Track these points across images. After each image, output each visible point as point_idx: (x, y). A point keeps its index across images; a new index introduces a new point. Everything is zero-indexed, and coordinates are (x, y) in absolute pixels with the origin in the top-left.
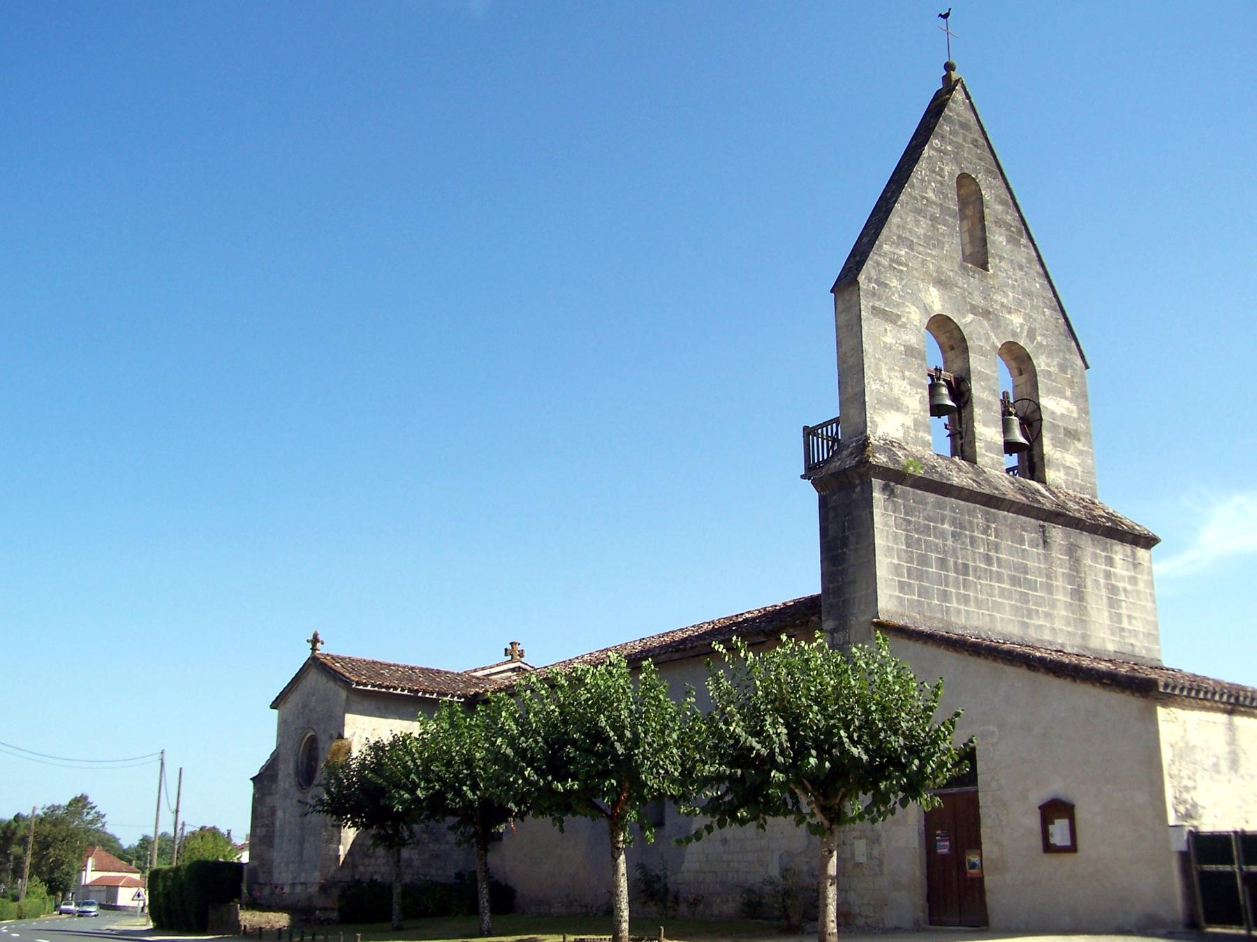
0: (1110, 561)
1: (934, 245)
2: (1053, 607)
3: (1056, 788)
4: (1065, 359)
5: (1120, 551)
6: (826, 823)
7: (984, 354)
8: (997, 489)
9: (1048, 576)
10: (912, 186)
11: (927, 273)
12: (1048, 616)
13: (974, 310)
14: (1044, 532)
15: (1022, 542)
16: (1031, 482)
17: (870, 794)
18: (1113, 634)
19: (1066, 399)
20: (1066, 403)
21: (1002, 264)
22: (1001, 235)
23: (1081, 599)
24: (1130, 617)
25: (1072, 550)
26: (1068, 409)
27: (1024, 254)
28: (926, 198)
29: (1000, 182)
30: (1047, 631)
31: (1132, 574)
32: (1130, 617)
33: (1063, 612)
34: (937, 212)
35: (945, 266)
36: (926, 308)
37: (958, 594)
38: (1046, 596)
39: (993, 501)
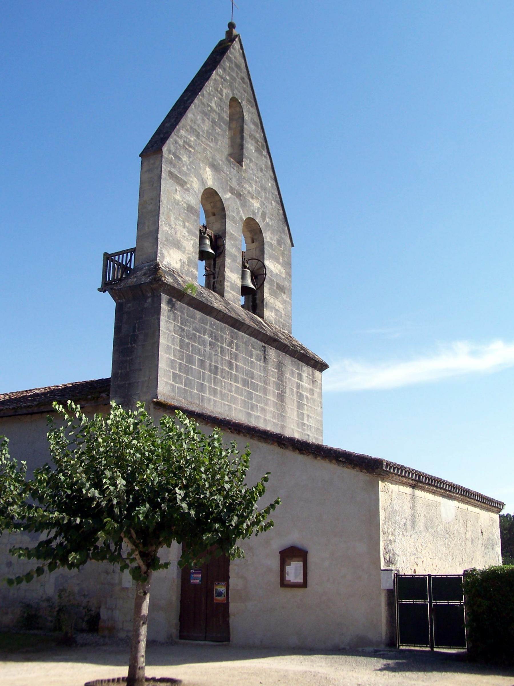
0: (300, 377)
1: (212, 140)
2: (266, 404)
3: (294, 538)
4: (280, 237)
5: (306, 371)
6: (144, 568)
7: (235, 222)
8: (239, 316)
9: (265, 383)
10: (203, 95)
11: (206, 158)
12: (263, 410)
13: (232, 190)
14: (265, 351)
15: (251, 356)
16: (255, 316)
17: (174, 542)
18: (298, 427)
19: (279, 263)
20: (279, 267)
21: (251, 165)
22: (252, 144)
23: (283, 401)
24: (308, 416)
25: (280, 366)
26: (280, 271)
27: (264, 162)
28: (211, 107)
29: (254, 110)
30: (262, 421)
31: (311, 387)
32: (308, 416)
33: (271, 408)
34: (216, 118)
35: (218, 156)
36: (203, 182)
37: (210, 388)
38: (263, 396)
39: (236, 324)
